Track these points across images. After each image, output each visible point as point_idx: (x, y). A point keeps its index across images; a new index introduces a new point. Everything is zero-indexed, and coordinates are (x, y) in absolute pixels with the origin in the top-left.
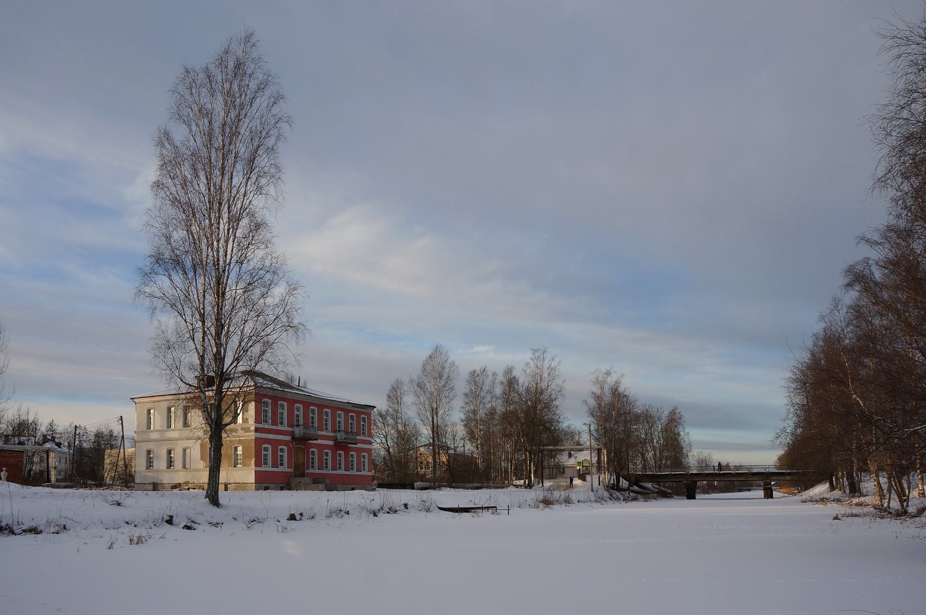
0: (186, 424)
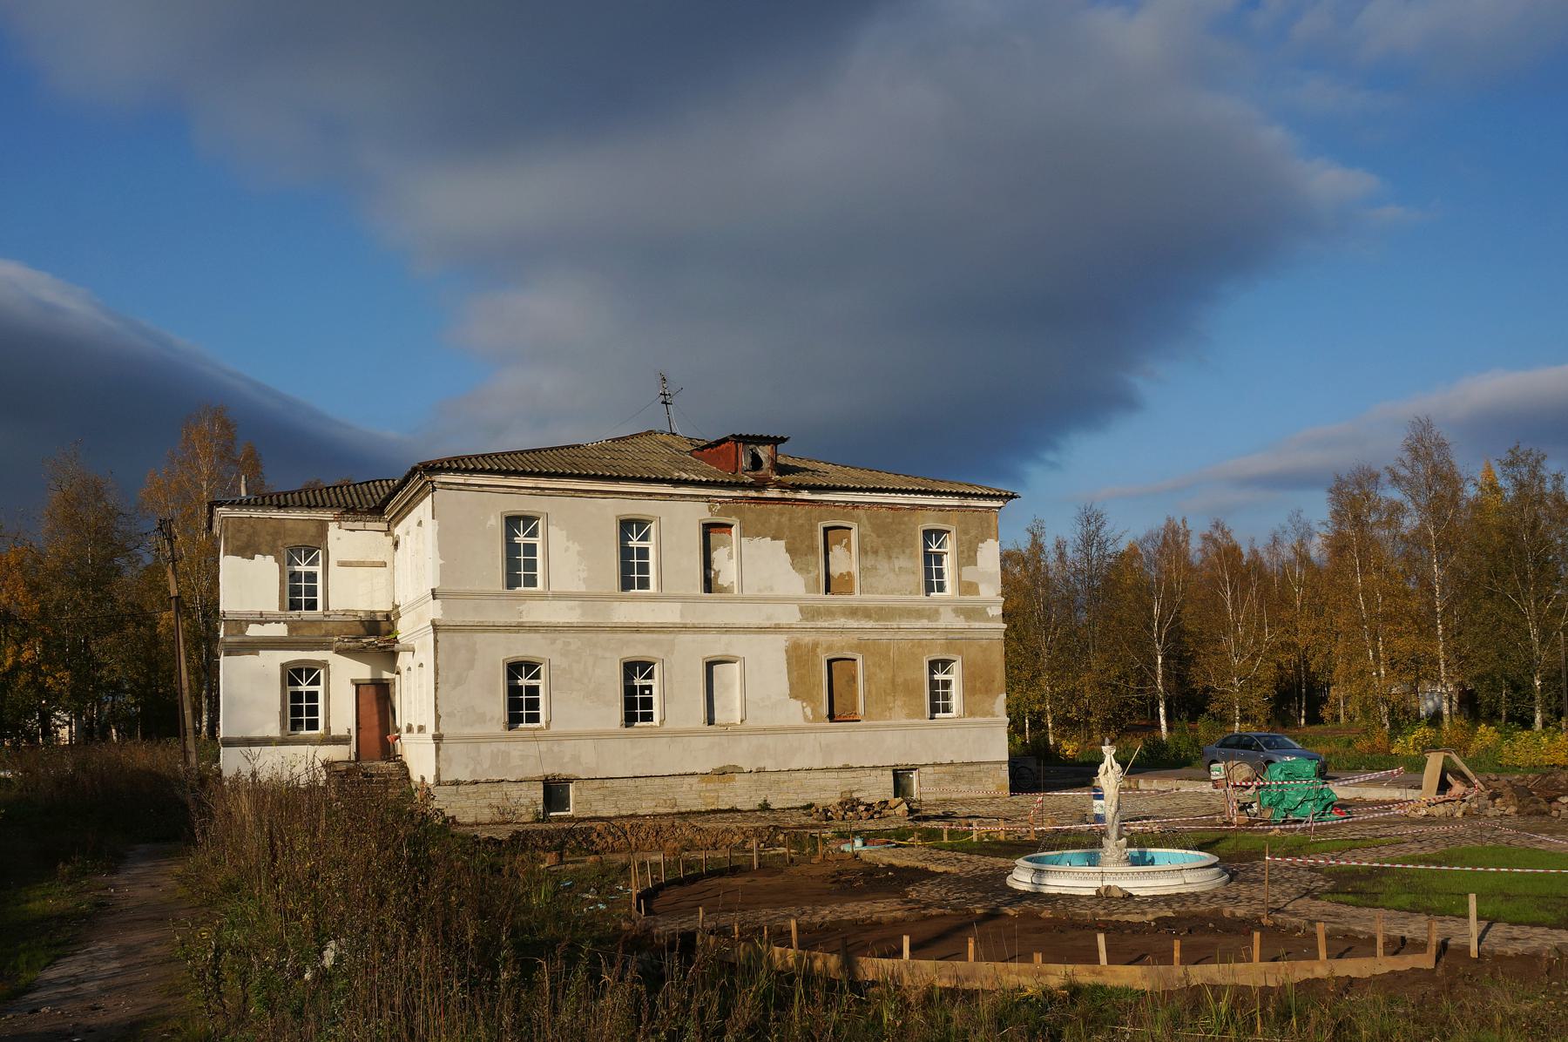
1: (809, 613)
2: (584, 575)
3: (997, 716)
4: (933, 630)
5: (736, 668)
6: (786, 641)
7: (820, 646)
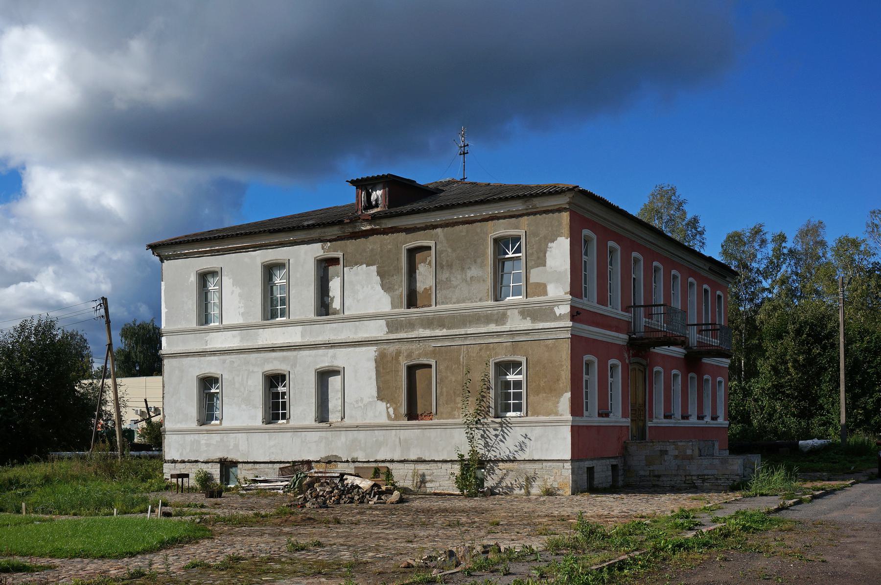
0: (324, 306)
1: (393, 325)
2: (242, 310)
3: (561, 415)
4: (498, 334)
6: (375, 351)
7: (402, 355)
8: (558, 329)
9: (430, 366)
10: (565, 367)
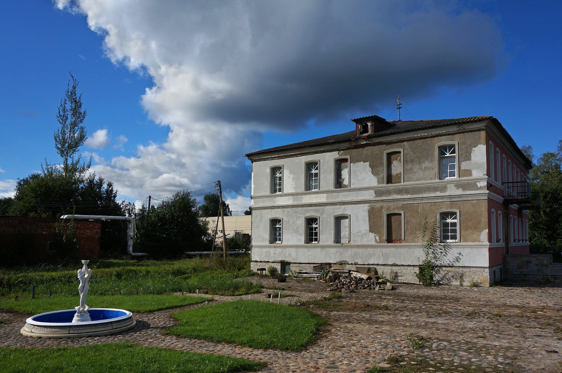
0: (339, 183)
1: (379, 193)
2: (294, 186)
3: (482, 242)
4: (442, 197)
5: (347, 220)
6: (368, 207)
8: (480, 195)
9: (400, 214)
10: (484, 215)
